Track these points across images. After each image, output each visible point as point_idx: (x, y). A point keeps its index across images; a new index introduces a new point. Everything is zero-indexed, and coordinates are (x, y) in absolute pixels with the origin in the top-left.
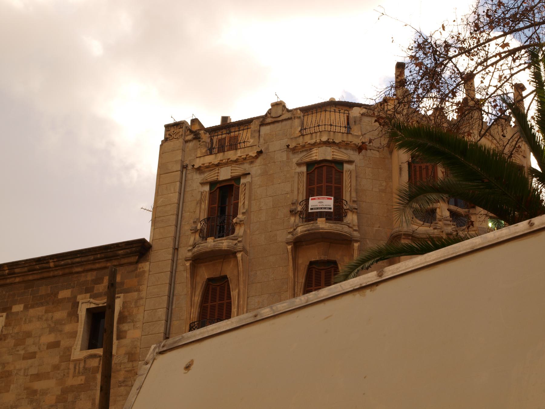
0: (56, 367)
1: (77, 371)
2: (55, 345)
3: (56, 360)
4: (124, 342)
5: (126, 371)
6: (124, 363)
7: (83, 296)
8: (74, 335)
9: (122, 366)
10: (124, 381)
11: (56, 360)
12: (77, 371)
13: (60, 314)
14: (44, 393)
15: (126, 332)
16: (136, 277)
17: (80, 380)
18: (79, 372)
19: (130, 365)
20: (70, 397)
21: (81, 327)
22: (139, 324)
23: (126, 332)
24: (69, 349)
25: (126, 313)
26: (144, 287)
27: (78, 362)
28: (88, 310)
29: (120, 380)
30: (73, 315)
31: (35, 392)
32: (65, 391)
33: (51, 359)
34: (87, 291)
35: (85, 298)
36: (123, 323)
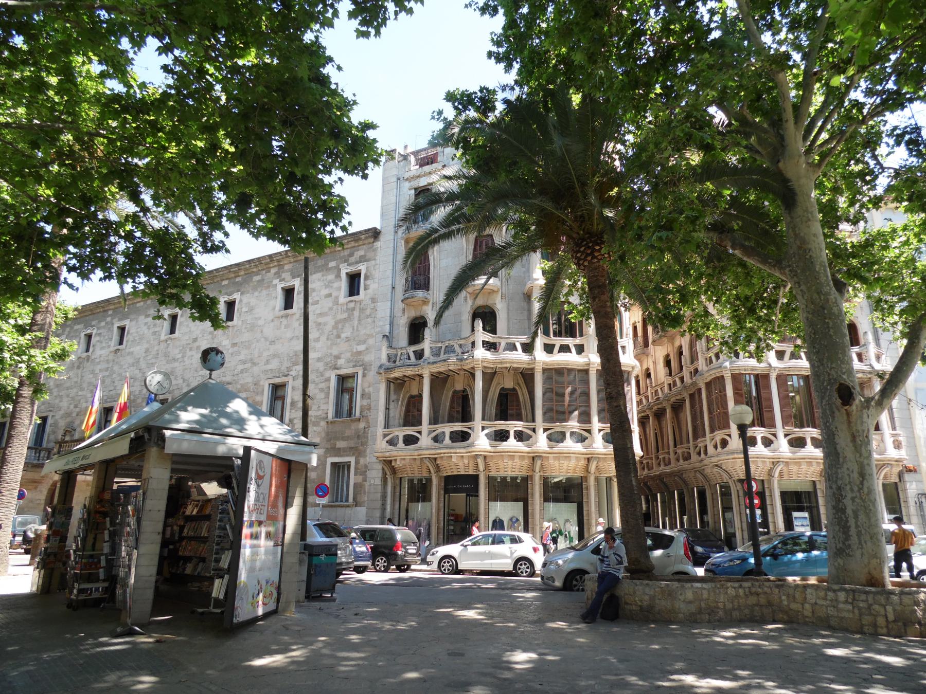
0: (331, 309)
2: (330, 295)
3: (330, 305)
4: (368, 291)
8: (339, 289)
11: (330, 305)
13: (331, 277)
14: (325, 324)
17: (345, 315)
20: (340, 326)
21: (344, 284)
22: (376, 280)
24: (337, 298)
30: (338, 276)
31: (320, 324)
32: (337, 323)
33: (328, 303)
34: (345, 262)
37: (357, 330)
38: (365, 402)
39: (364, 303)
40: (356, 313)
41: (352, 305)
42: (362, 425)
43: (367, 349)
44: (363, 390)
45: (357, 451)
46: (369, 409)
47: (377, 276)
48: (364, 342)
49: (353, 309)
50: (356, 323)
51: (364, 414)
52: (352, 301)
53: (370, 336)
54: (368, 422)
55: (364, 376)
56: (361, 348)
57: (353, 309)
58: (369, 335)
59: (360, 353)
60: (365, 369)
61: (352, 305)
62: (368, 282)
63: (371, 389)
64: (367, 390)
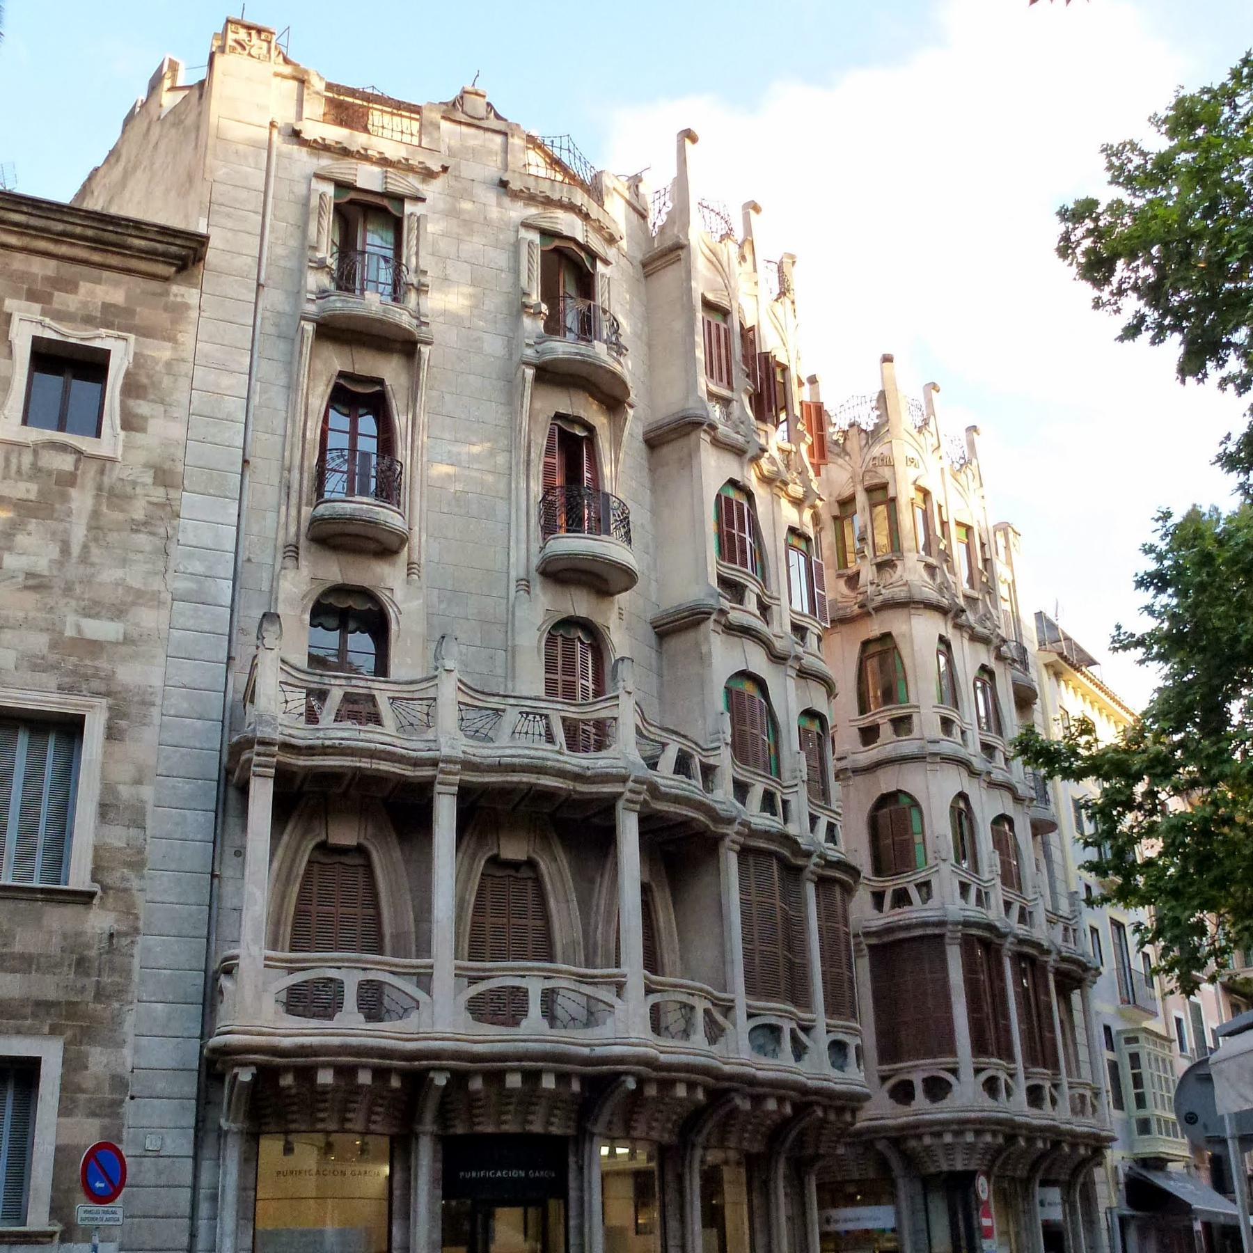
1: (14, 467)
5: (150, 503)
6: (145, 485)
7: (24, 304)
9: (139, 490)
10: (145, 524)
12: (14, 467)
15: (145, 419)
16: (166, 309)
17: (27, 490)
18: (19, 471)
19: (159, 494)
23: (145, 419)
25: (144, 380)
26: (186, 338)
27: (16, 448)
28: (36, 341)
29: (136, 517)
34: (32, 296)
35: (28, 311)
36: (138, 397)
37: (84, 558)
38: (117, 836)
39: (117, 472)
40: (81, 500)
41: (65, 463)
42: (99, 921)
43: (127, 640)
44: (108, 788)
45: (79, 1023)
46: (137, 865)
47: (181, 396)
48: (118, 612)
49: (69, 480)
50: (79, 533)
51: (112, 879)
52: (63, 448)
53: (140, 597)
54: (129, 911)
55: (112, 734)
56: (102, 629)
57: (69, 480)
58: (139, 594)
59: (95, 647)
60: (116, 713)
61: (65, 463)
62: (142, 407)
63: (147, 792)
64: (125, 791)
